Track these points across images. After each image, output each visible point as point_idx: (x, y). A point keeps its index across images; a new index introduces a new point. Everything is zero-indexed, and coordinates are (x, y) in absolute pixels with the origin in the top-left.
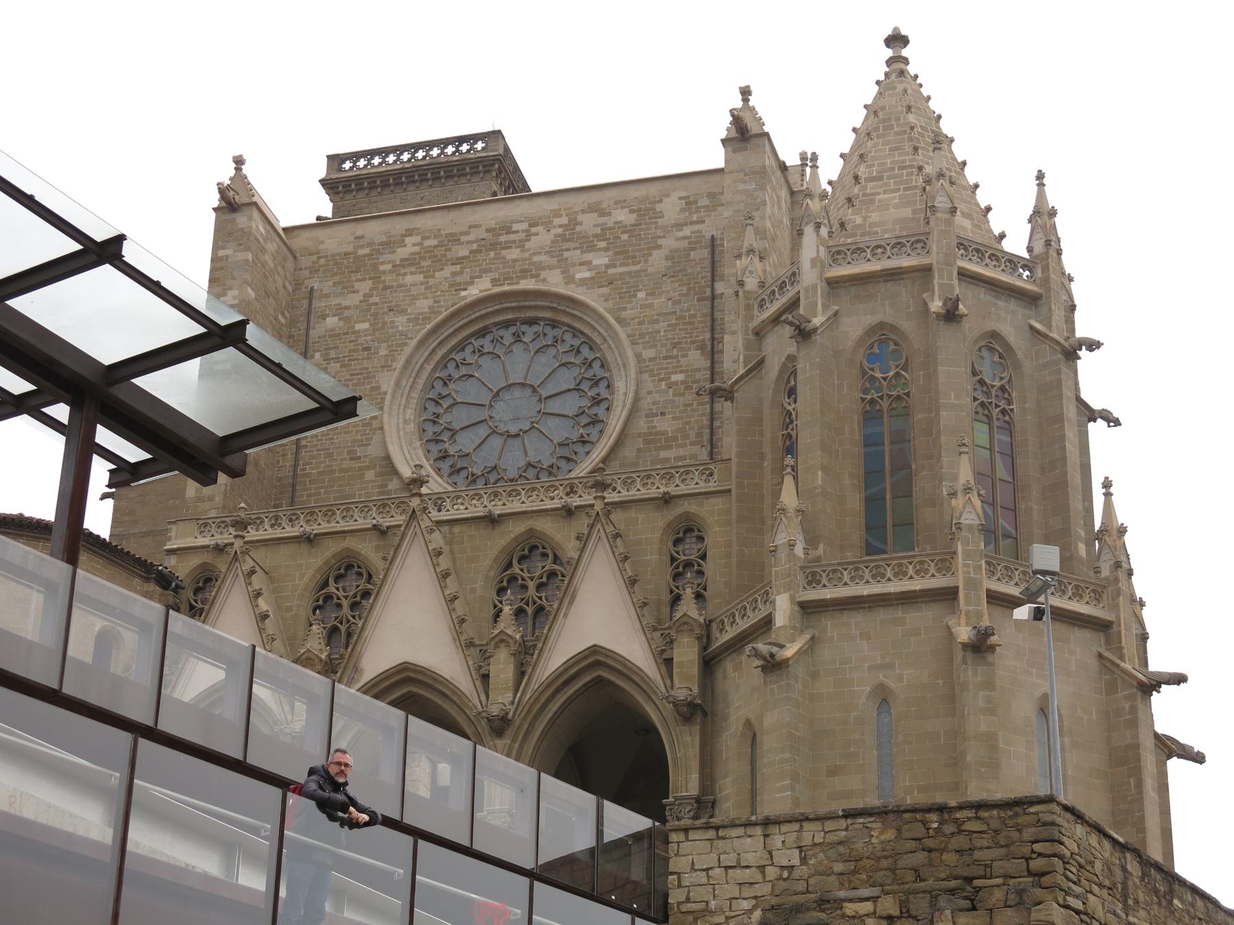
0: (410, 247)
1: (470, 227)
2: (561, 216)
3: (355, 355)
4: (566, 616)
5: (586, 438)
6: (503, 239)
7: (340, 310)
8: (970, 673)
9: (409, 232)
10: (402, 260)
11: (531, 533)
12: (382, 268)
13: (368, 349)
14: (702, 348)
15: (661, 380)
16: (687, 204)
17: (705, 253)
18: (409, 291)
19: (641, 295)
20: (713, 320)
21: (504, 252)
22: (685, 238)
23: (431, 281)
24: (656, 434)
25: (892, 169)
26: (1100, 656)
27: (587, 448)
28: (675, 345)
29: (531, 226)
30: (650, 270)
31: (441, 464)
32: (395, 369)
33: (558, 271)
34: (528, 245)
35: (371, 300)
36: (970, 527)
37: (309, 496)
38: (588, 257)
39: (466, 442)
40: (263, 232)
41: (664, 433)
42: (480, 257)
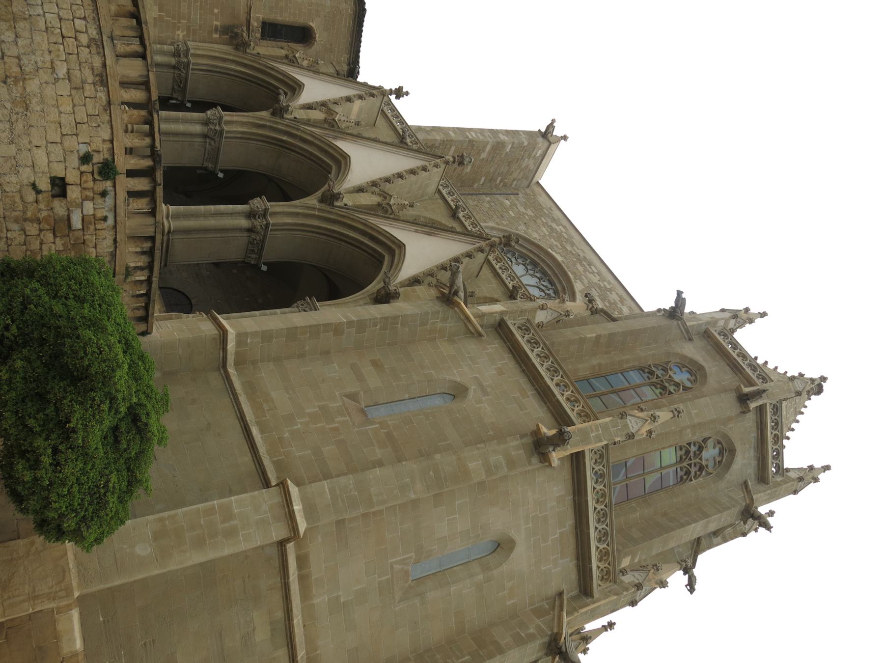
1: (582, 250)
4: (417, 231)
6: (584, 263)
7: (513, 205)
8: (515, 443)
9: (564, 227)
23: (548, 237)
26: (560, 594)
35: (526, 216)
36: (626, 426)
40: (538, 155)
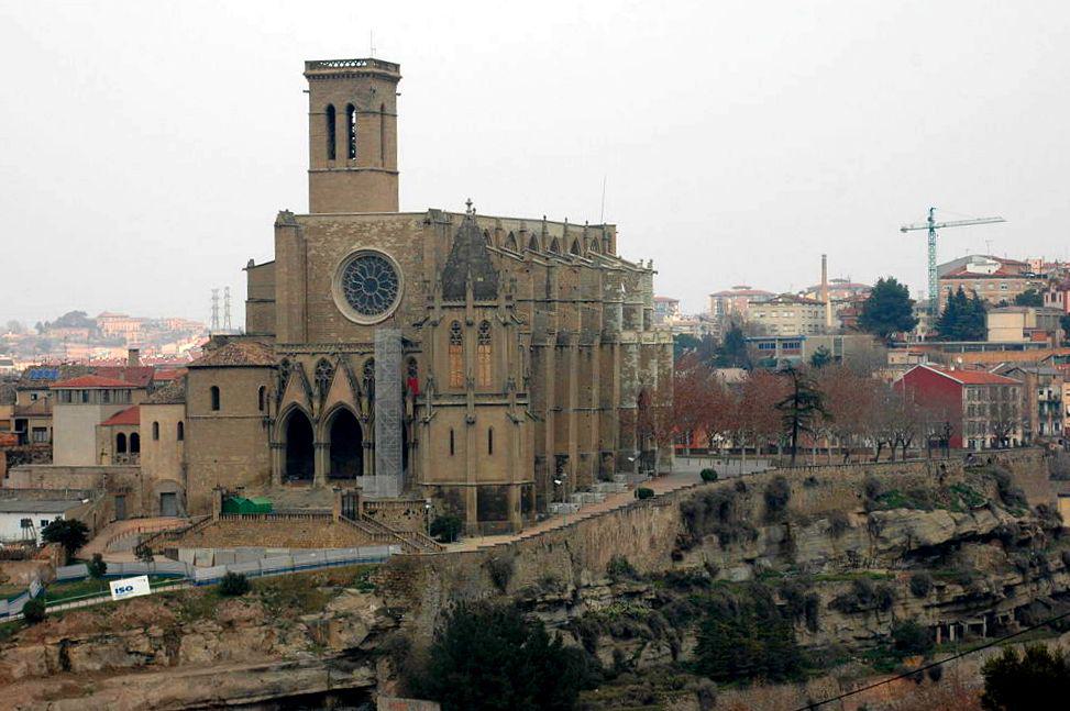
0: (335, 228)
7: (315, 248)
9: (334, 222)
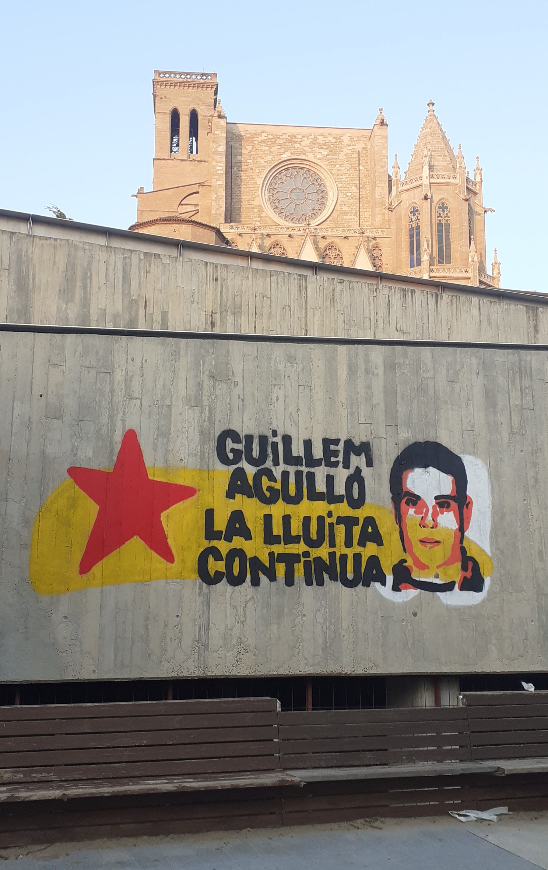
0: (263, 137)
1: (283, 134)
2: (311, 135)
3: (248, 170)
5: (320, 208)
9: (263, 132)
10: (261, 141)
11: (332, 242)
12: (255, 142)
13: (252, 169)
14: (356, 186)
15: (344, 194)
16: (351, 138)
17: (357, 156)
18: (264, 152)
19: (338, 166)
20: (359, 178)
21: (294, 144)
22: (350, 150)
24: (343, 211)
25: (438, 149)
27: (320, 211)
28: (348, 184)
29: (302, 137)
30: (340, 158)
31: (275, 210)
32: (262, 177)
33: (312, 154)
34: (302, 143)
37: (236, 214)
38: (321, 151)
39: (283, 204)
41: (346, 211)
42: (287, 144)
